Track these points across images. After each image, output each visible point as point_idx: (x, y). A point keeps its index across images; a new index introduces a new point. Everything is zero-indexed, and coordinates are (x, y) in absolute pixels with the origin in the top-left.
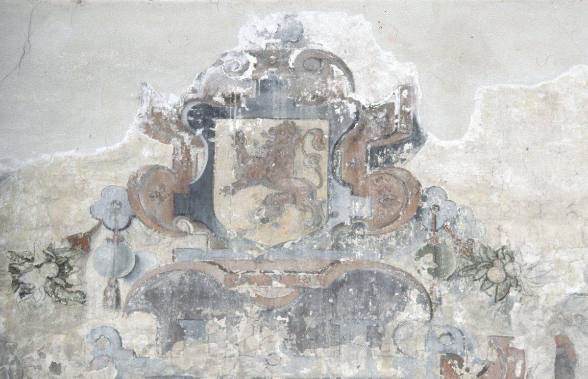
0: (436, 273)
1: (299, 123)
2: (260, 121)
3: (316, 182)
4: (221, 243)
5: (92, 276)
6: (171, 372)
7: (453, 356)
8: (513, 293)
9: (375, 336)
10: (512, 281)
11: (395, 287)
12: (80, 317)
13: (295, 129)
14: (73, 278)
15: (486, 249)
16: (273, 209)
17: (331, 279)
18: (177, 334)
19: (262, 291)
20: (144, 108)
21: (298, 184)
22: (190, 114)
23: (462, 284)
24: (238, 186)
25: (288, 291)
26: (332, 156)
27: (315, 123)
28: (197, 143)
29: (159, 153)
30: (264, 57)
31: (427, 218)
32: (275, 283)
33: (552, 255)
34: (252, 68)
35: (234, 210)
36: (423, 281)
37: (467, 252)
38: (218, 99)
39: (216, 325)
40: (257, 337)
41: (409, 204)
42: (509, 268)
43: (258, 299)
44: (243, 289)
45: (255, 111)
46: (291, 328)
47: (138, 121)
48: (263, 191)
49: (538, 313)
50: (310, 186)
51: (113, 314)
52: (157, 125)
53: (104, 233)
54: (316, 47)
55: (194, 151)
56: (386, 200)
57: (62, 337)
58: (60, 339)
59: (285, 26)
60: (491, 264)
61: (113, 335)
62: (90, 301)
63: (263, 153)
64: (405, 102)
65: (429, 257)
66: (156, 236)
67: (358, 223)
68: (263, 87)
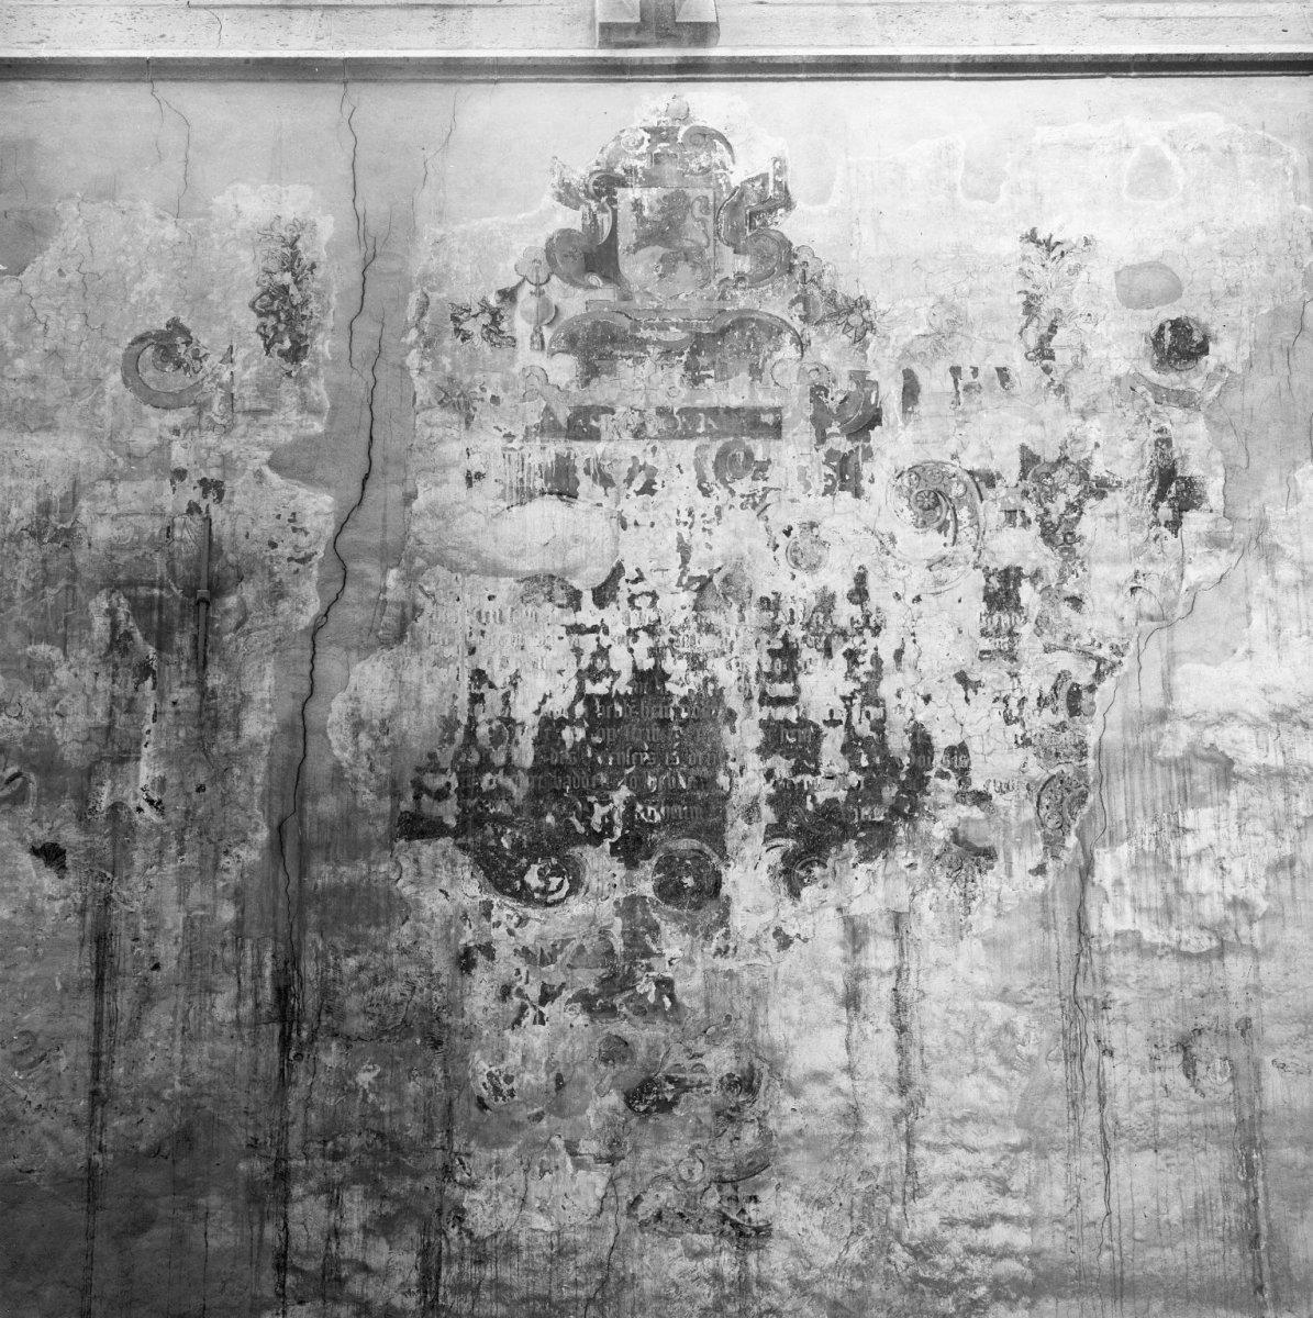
0: (805, 319)
1: (689, 192)
2: (654, 191)
3: (704, 242)
4: (626, 298)
5: (520, 324)
6: (589, 403)
7: (820, 387)
8: (869, 335)
9: (756, 372)
10: (869, 326)
11: (774, 330)
12: (512, 359)
13: (686, 197)
14: (504, 326)
15: (846, 299)
16: (668, 265)
17: (719, 325)
18: (590, 372)
19: (662, 336)
20: (556, 180)
21: (688, 244)
22: (595, 184)
23: (827, 328)
24: (638, 246)
25: (684, 335)
26: (716, 221)
27: (699, 192)
28: (603, 210)
29: (572, 219)
30: (656, 133)
31: (798, 274)
32: (673, 329)
33: (900, 304)
34: (646, 144)
35: (638, 268)
36: (794, 326)
37: (831, 300)
38: (619, 171)
39: (625, 367)
40: (660, 374)
41: (783, 261)
42: (866, 314)
43: (658, 343)
44: (644, 334)
45: (650, 181)
46: (687, 368)
47: (552, 190)
48: (660, 250)
49: (889, 352)
50: (699, 246)
51: (538, 355)
52: (567, 195)
53: (528, 288)
54: (701, 124)
55: (599, 216)
56: (762, 257)
57: (499, 375)
58: (496, 378)
59: (675, 105)
60: (851, 311)
61: (540, 373)
62: (519, 345)
63: (659, 218)
64: (779, 172)
65: (800, 306)
66: (571, 289)
67: (741, 277)
68: (657, 159)
